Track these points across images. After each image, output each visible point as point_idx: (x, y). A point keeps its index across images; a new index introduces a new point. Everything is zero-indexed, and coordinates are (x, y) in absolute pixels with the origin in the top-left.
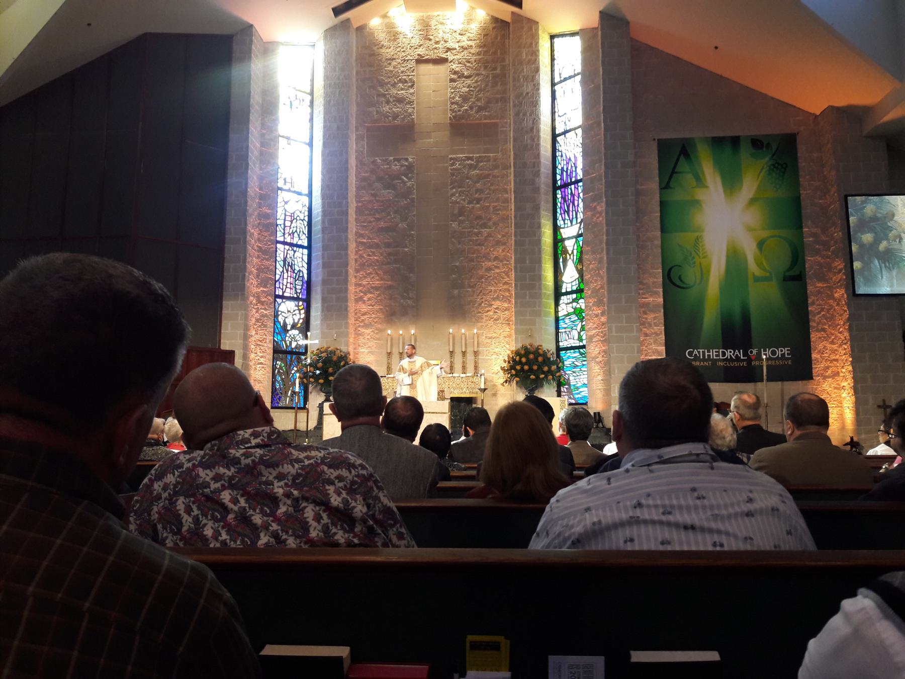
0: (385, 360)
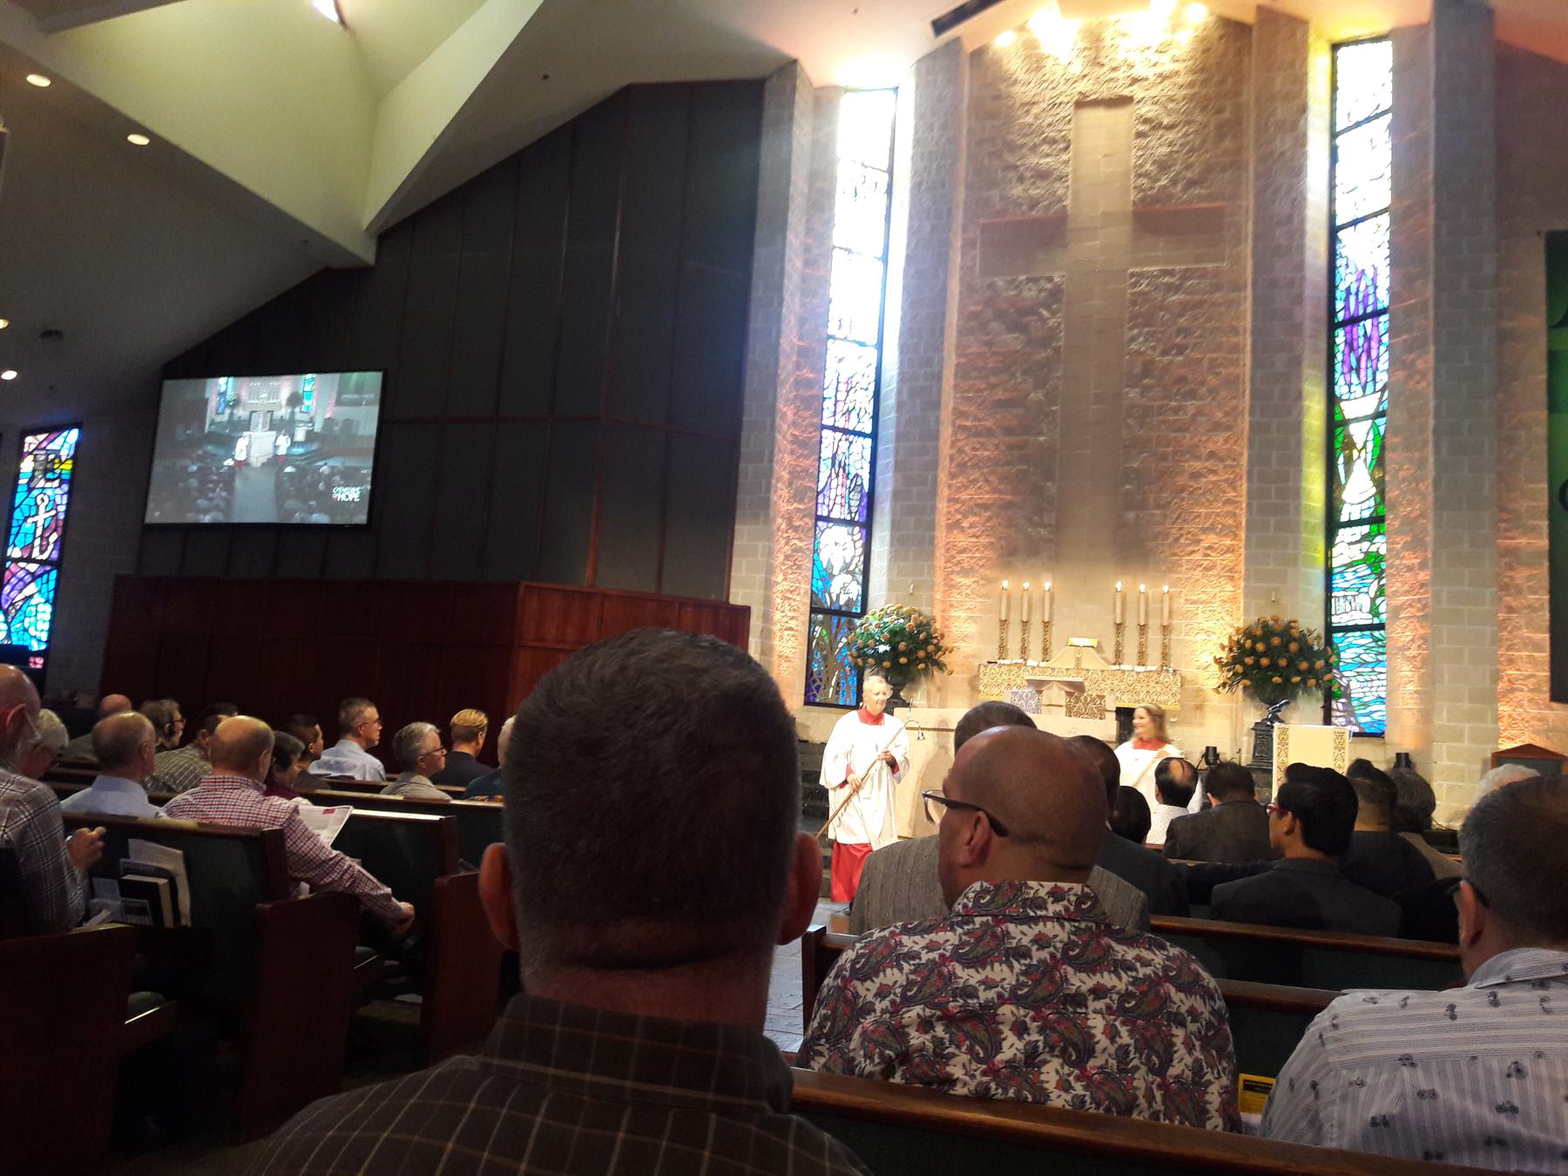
0: (997, 631)
